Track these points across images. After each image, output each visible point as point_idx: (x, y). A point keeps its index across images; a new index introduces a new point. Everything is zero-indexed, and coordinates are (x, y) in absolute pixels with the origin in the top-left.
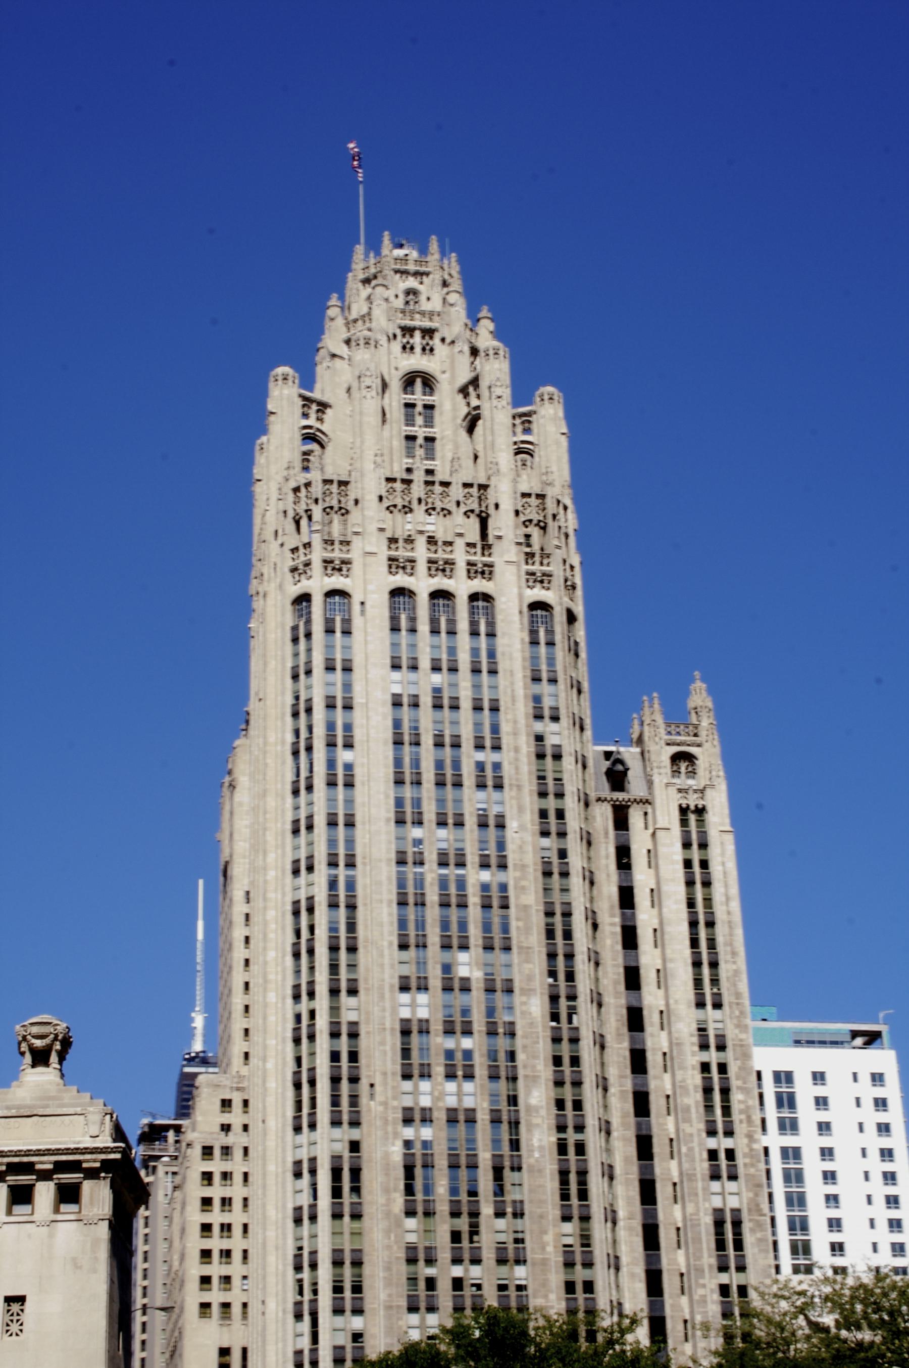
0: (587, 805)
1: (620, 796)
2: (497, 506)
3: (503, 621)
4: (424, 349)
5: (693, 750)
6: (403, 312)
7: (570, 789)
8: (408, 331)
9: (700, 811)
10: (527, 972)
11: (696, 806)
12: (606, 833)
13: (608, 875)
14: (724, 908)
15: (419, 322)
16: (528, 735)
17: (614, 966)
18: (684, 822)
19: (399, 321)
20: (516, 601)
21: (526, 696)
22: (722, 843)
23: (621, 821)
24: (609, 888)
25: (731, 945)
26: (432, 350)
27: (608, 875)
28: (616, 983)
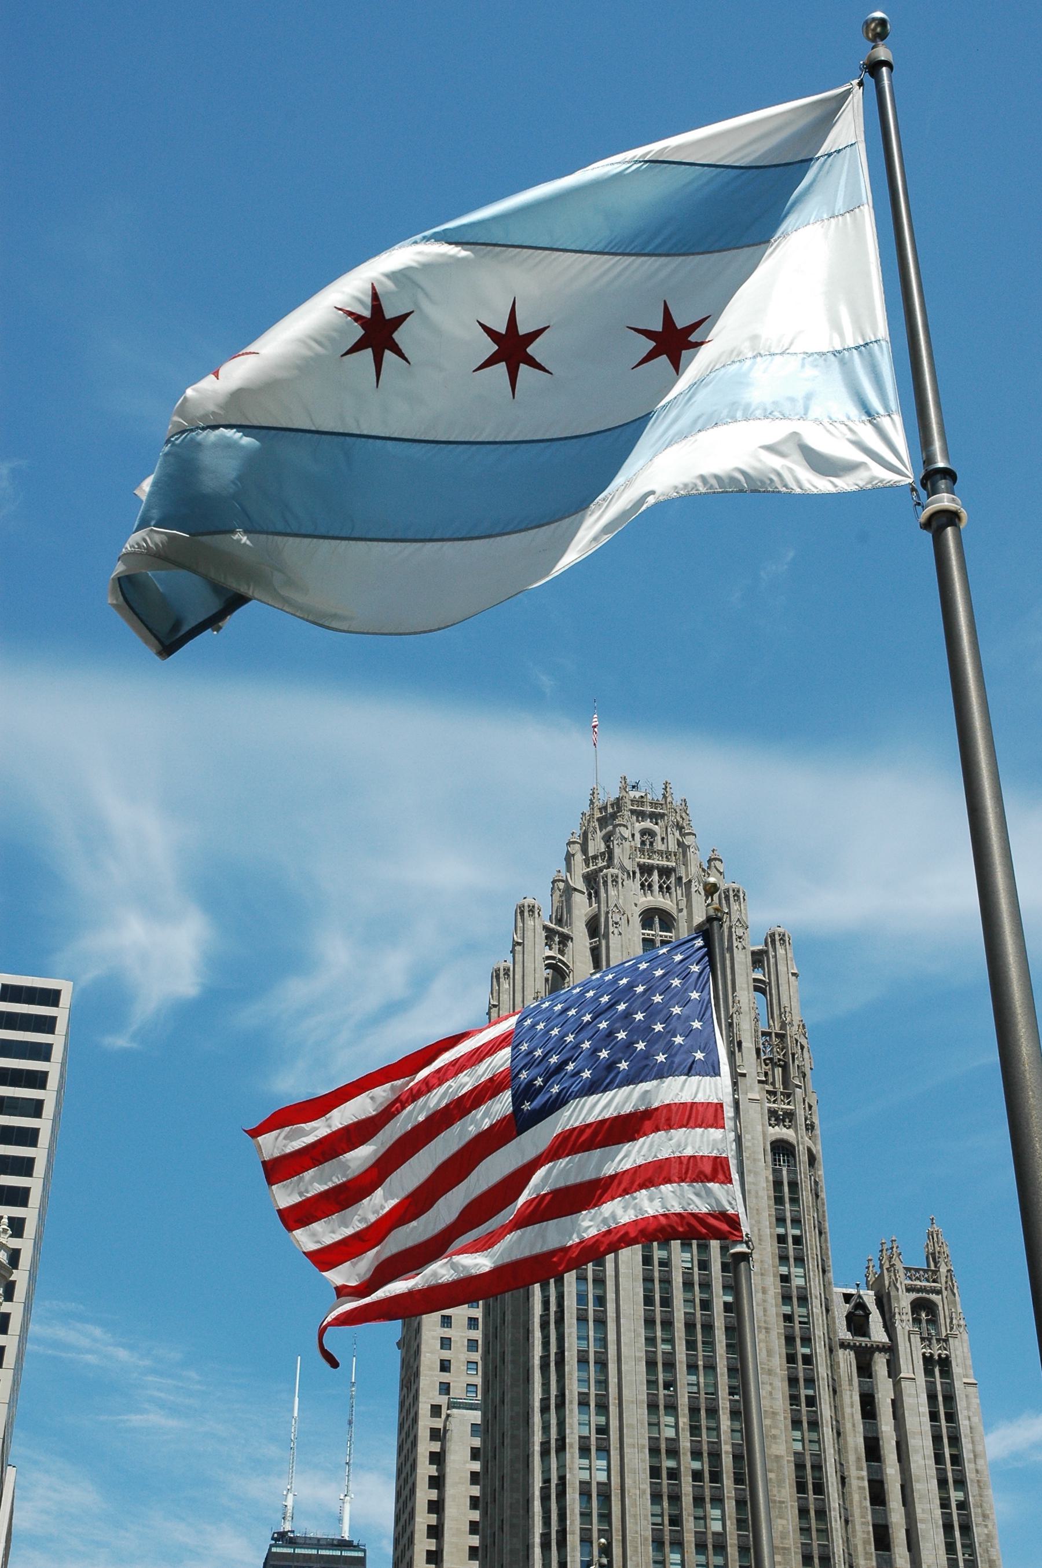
0: (831, 1351)
1: (862, 1340)
2: (740, 1043)
3: (748, 1158)
4: (661, 887)
5: (933, 1297)
6: (642, 851)
7: (819, 1332)
8: (646, 870)
9: (945, 1363)
10: (780, 1528)
11: (940, 1355)
12: (851, 1380)
13: (854, 1425)
14: (972, 1466)
15: (656, 861)
16: (774, 1276)
17: (863, 1523)
18: (929, 1372)
19: (638, 860)
20: (761, 1139)
21: (771, 1236)
22: (967, 1396)
23: (865, 1369)
24: (856, 1441)
25: (981, 1506)
26: (668, 888)
27: (854, 1425)
28: (866, 1542)
